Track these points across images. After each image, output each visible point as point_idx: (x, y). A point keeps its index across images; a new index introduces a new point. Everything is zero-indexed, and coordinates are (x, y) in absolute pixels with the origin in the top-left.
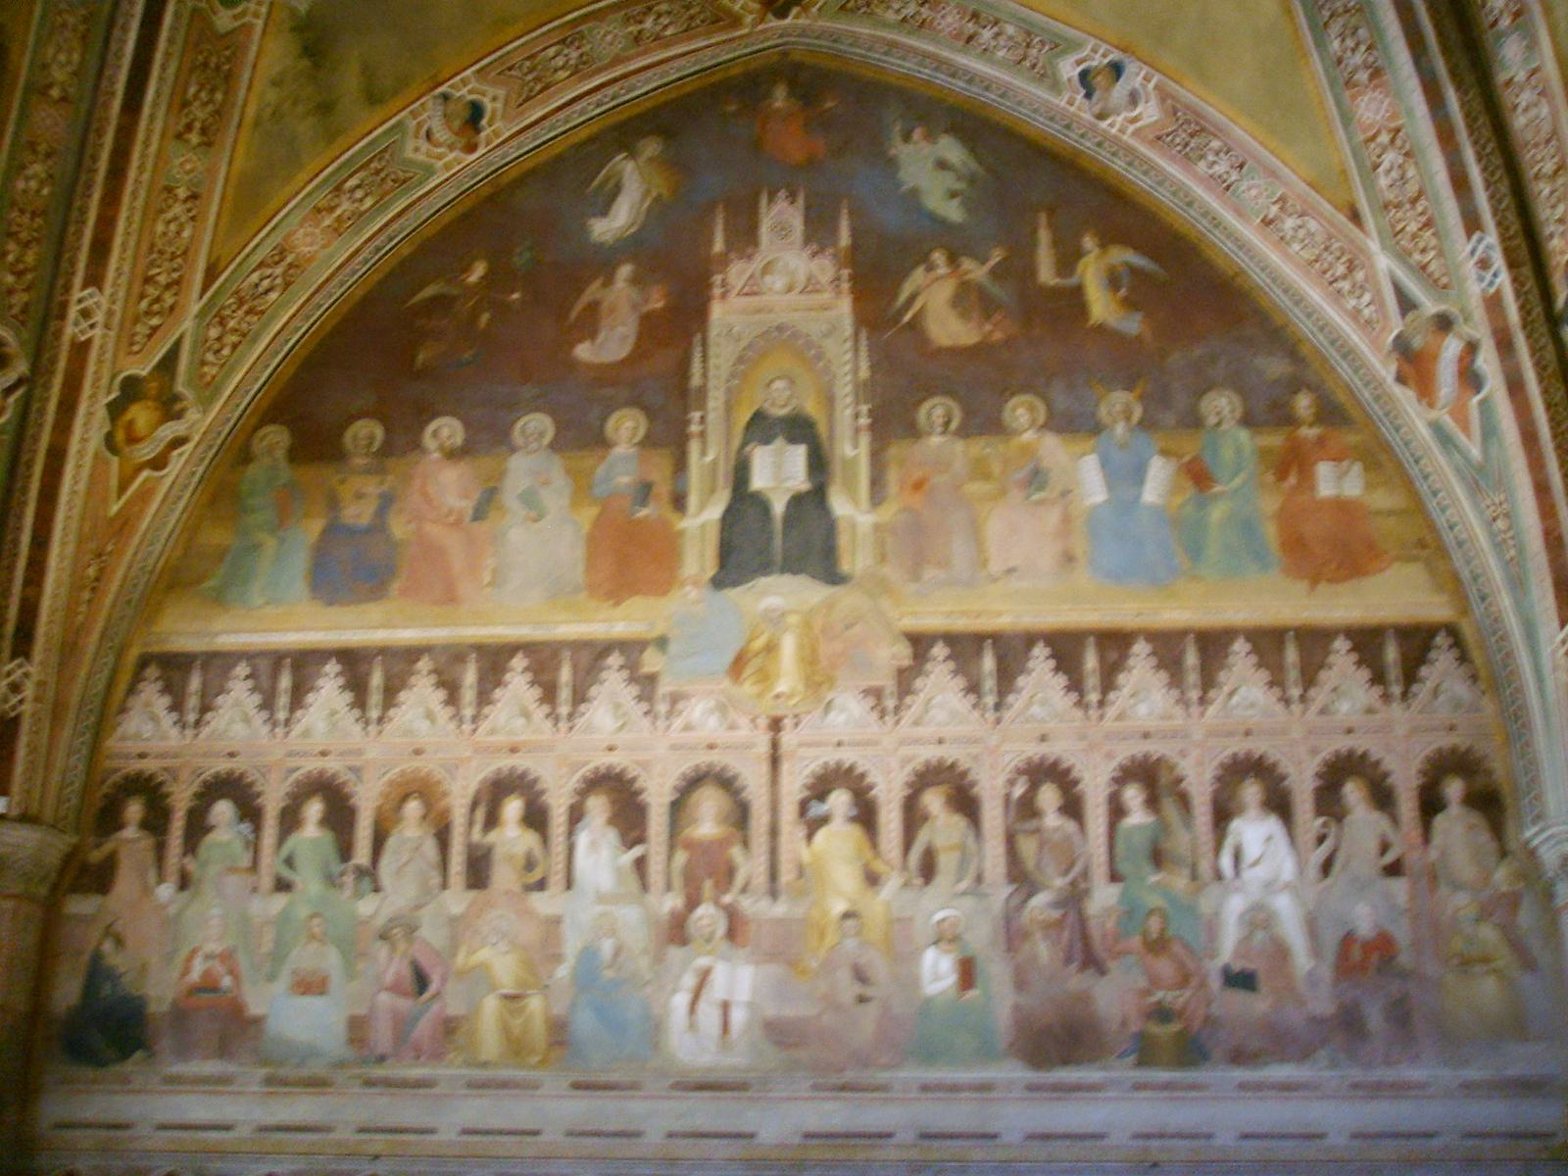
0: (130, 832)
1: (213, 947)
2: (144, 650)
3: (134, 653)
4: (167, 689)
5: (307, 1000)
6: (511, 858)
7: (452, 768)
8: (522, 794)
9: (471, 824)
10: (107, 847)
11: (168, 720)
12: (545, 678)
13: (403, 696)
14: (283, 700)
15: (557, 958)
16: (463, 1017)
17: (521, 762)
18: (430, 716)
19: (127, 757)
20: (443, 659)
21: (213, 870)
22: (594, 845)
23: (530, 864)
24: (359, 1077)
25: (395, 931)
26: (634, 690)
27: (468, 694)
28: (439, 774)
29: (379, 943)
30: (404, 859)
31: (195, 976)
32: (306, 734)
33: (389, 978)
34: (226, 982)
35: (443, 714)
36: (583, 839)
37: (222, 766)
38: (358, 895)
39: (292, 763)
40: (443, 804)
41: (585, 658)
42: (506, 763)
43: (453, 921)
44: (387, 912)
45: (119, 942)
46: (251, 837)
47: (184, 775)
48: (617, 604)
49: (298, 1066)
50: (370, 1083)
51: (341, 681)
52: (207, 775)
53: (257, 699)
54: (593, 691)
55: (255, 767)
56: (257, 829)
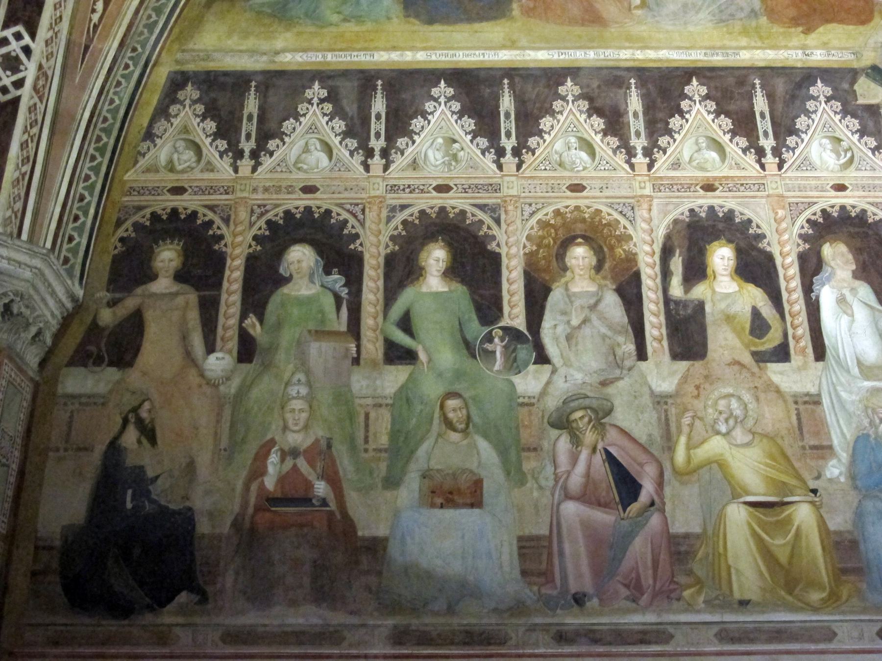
0: (163, 284)
1: (295, 439)
2: (178, 68)
3: (161, 76)
4: (211, 111)
5: (449, 514)
6: (729, 319)
7: (629, 208)
8: (730, 241)
9: (666, 274)
10: (130, 303)
11: (212, 150)
12: (732, 107)
13: (546, 123)
14: (377, 126)
15: (824, 450)
16: (698, 536)
17: (722, 201)
18: (588, 147)
19: (155, 191)
20: (595, 84)
21: (287, 336)
22: (841, 301)
23: (759, 326)
24: (546, 628)
25: (578, 414)
26: (855, 124)
27: (636, 124)
28: (609, 214)
29: (554, 433)
30: (575, 322)
31: (270, 483)
32: (414, 165)
33: (576, 480)
34: (321, 488)
35: (605, 146)
36: (827, 296)
37: (298, 202)
38: (514, 366)
39: (394, 200)
40: (619, 251)
41: (781, 86)
42: (702, 201)
43: (660, 400)
44: (561, 387)
45: (149, 433)
46: (344, 292)
47: (243, 215)
48: (808, 31)
49: (450, 610)
50: (562, 637)
51: (456, 106)
52: (276, 214)
53: (339, 125)
54: (801, 122)
55: (340, 205)
56: (354, 281)
